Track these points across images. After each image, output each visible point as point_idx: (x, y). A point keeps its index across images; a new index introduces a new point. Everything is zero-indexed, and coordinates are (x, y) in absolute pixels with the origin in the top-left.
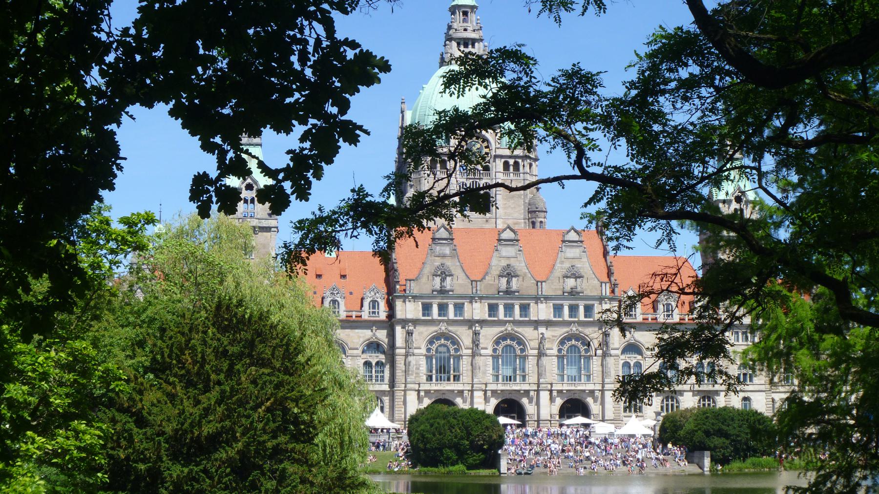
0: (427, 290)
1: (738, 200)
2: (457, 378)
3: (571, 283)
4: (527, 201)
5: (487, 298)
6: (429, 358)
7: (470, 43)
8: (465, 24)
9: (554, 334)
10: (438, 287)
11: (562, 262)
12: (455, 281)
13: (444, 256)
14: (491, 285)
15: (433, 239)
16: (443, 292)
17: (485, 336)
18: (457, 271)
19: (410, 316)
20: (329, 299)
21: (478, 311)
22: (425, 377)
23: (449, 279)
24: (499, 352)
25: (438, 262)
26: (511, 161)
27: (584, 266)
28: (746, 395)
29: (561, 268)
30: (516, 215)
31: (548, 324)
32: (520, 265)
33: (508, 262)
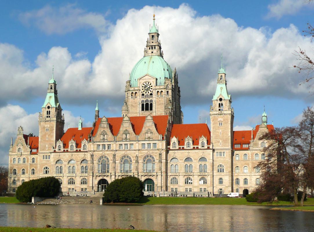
0: (98, 140)
1: (221, 100)
2: (108, 172)
5: (118, 141)
7: (153, 47)
8: (153, 40)
11: (145, 128)
13: (104, 128)
14: (120, 137)
17: (118, 156)
19: (92, 150)
20: (71, 144)
23: (106, 136)
24: (123, 162)
25: (102, 130)
30: (161, 111)
33: (126, 129)
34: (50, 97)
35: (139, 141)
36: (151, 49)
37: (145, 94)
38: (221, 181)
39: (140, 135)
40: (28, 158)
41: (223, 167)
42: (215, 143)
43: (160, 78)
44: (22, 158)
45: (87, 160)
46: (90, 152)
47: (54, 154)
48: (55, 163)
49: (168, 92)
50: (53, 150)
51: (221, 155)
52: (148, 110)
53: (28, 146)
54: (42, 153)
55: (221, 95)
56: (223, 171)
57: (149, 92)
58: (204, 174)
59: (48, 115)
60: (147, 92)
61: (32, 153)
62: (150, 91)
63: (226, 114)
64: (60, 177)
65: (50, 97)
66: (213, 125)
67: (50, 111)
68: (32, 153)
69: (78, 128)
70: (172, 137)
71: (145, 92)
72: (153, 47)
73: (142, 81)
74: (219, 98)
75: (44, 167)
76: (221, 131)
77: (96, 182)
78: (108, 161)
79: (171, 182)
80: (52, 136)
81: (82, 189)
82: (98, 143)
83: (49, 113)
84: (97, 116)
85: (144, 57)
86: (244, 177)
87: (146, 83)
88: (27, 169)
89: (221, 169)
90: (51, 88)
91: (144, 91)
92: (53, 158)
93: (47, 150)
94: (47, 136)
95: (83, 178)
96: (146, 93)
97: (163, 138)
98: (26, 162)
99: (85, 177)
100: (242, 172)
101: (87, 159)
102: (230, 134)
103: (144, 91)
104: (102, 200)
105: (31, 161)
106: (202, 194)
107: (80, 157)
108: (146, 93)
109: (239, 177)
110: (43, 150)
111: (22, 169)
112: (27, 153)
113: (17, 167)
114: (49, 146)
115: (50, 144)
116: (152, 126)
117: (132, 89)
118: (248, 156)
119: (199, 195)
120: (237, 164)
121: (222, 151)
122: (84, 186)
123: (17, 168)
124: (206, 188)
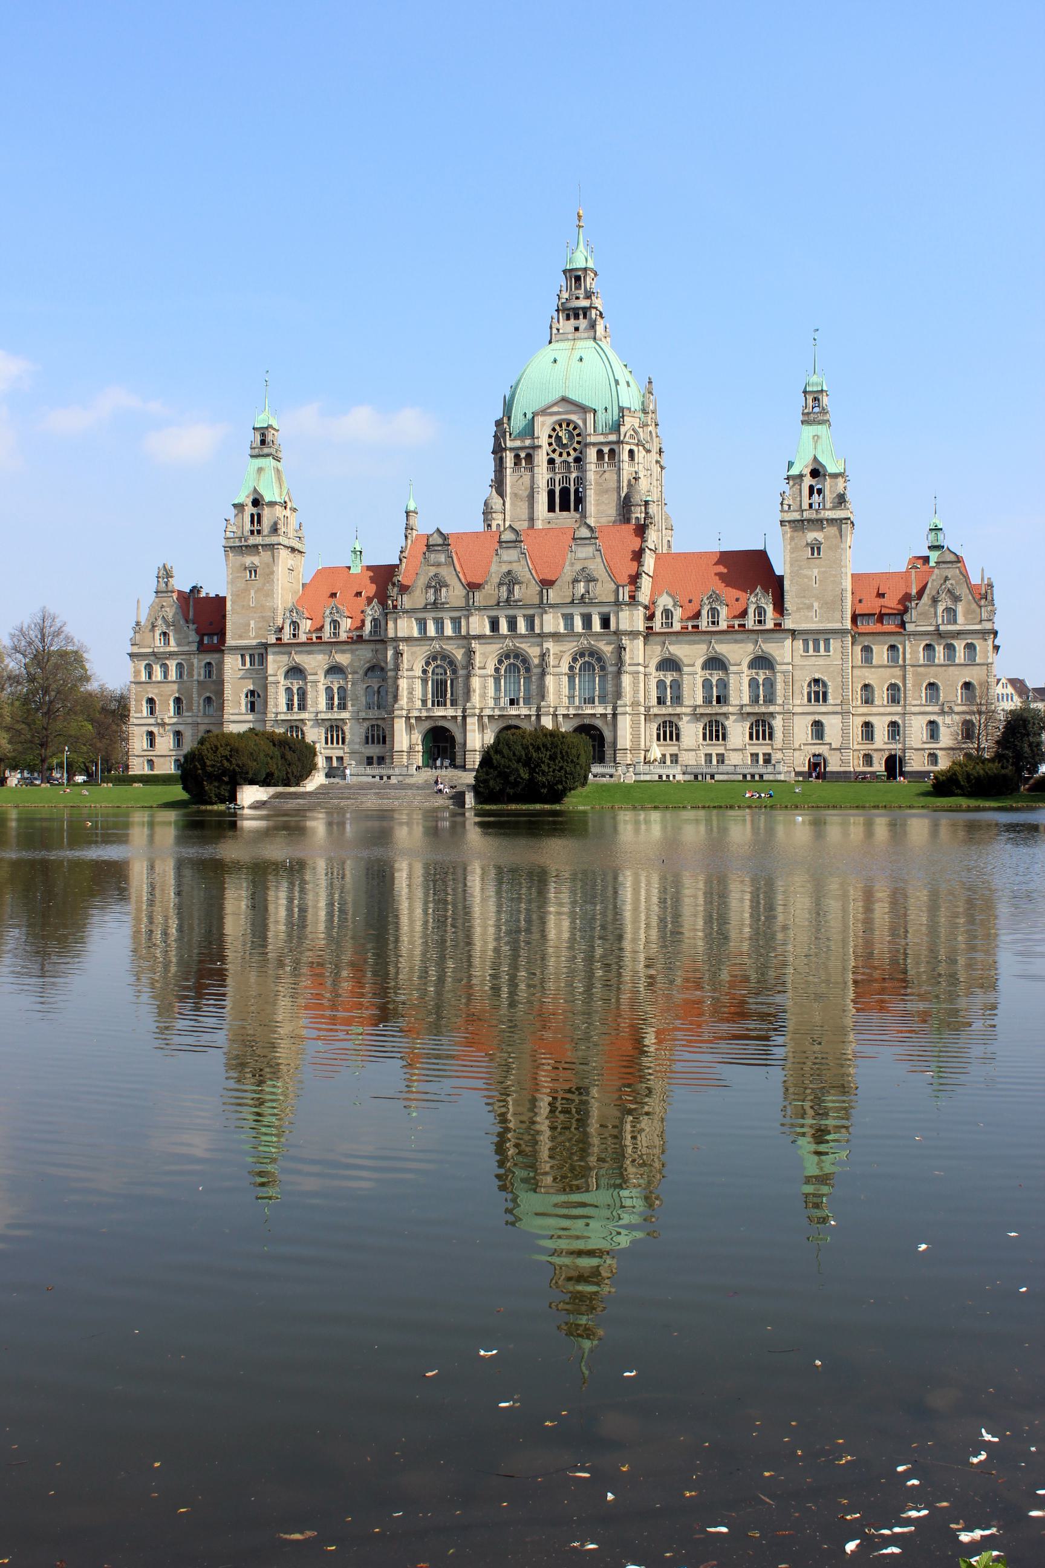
1: (815, 473)
3: (581, 588)
4: (623, 495)
5: (485, 608)
6: (425, 681)
7: (581, 312)
9: (561, 649)
10: (432, 598)
11: (572, 564)
12: (451, 593)
13: (439, 565)
15: (428, 546)
16: (436, 606)
18: (452, 580)
21: (479, 624)
22: (420, 703)
23: (444, 590)
25: (433, 571)
26: (606, 450)
27: (597, 567)
28: (817, 718)
29: (568, 572)
31: (555, 636)
32: (522, 570)
34: (260, 470)
35: (552, 606)
36: (572, 317)
37: (558, 460)
38: (818, 728)
39: (556, 586)
40: (193, 665)
41: (825, 685)
42: (798, 610)
43: (606, 409)
44: (172, 664)
45: (382, 669)
46: (395, 644)
47: (276, 649)
48: (281, 678)
49: (631, 452)
50: (272, 640)
51: (817, 649)
52: (569, 510)
53: (193, 627)
54: (236, 648)
55: (815, 459)
56: (825, 700)
57: (572, 452)
58: (763, 709)
59: (256, 528)
60: (565, 455)
61: (202, 648)
62: (575, 450)
63: (832, 520)
64: (297, 723)
65: (260, 470)
66: (792, 553)
67: (259, 515)
68: (202, 648)
69: (349, 568)
70: (660, 595)
71: (557, 453)
72: (581, 312)
73: (550, 420)
74: (807, 471)
75: (245, 690)
76: (816, 571)
77: (417, 737)
78: (454, 672)
79: (658, 735)
80: (270, 594)
81: (368, 758)
82: (420, 615)
83: (256, 519)
84: (409, 528)
85: (550, 342)
86: (889, 719)
87: (561, 426)
88: (190, 699)
89: (817, 693)
90: (263, 442)
91: (554, 451)
92: (274, 661)
93: (254, 638)
94: (252, 593)
95: (373, 726)
96: (561, 455)
97: (632, 597)
98: (185, 678)
99: (379, 722)
100: (880, 704)
101: (383, 664)
102: (848, 584)
103: (554, 451)
104: (472, 794)
105: (202, 672)
106: (763, 770)
107: (360, 660)
108: (561, 455)
109: (872, 719)
110: (241, 637)
111: (172, 699)
112: (186, 648)
113: (156, 691)
114: (260, 625)
115: (263, 617)
116: (594, 557)
117: (518, 443)
118: (901, 650)
119: (753, 776)
120: (865, 678)
121: (822, 637)
122: (374, 750)
123: (157, 695)
124: (769, 754)
